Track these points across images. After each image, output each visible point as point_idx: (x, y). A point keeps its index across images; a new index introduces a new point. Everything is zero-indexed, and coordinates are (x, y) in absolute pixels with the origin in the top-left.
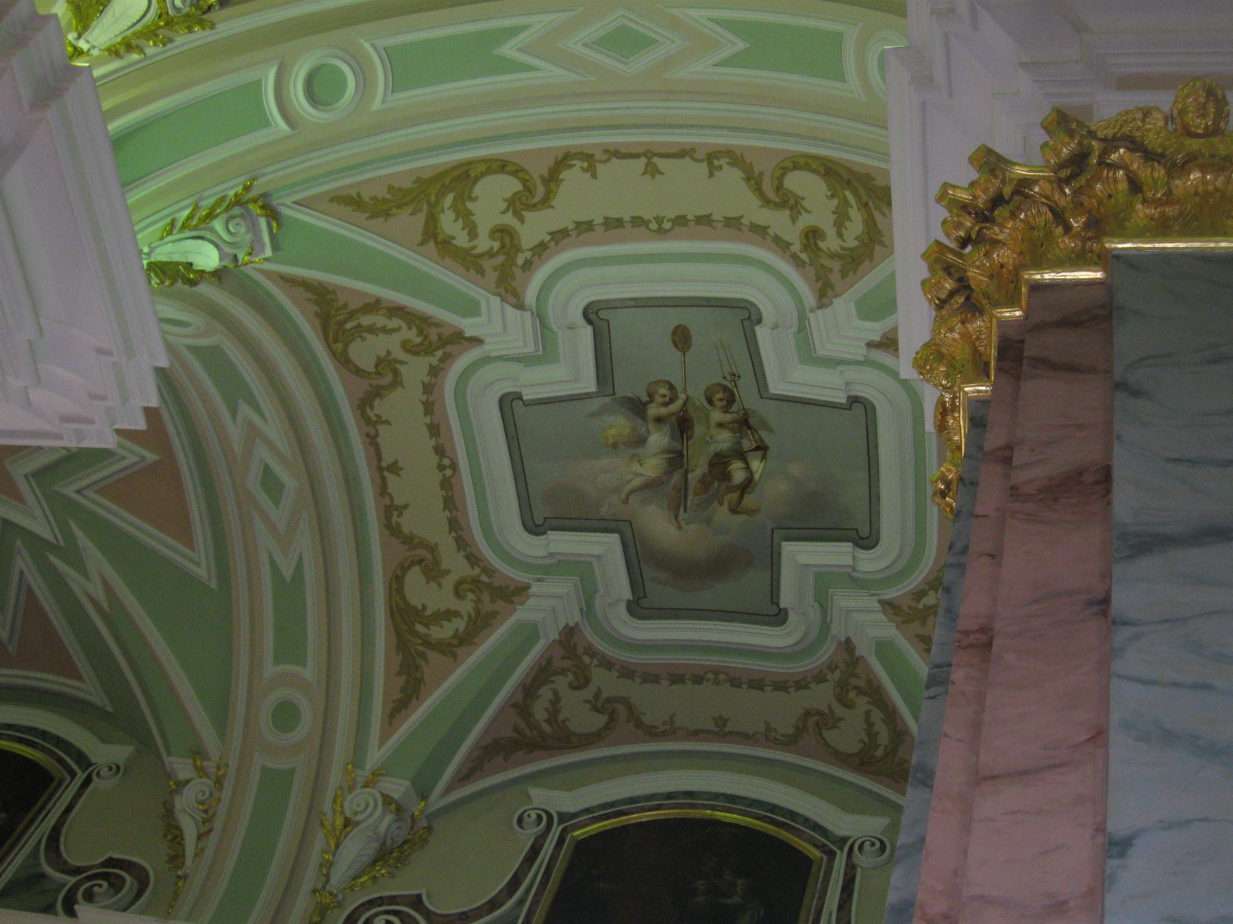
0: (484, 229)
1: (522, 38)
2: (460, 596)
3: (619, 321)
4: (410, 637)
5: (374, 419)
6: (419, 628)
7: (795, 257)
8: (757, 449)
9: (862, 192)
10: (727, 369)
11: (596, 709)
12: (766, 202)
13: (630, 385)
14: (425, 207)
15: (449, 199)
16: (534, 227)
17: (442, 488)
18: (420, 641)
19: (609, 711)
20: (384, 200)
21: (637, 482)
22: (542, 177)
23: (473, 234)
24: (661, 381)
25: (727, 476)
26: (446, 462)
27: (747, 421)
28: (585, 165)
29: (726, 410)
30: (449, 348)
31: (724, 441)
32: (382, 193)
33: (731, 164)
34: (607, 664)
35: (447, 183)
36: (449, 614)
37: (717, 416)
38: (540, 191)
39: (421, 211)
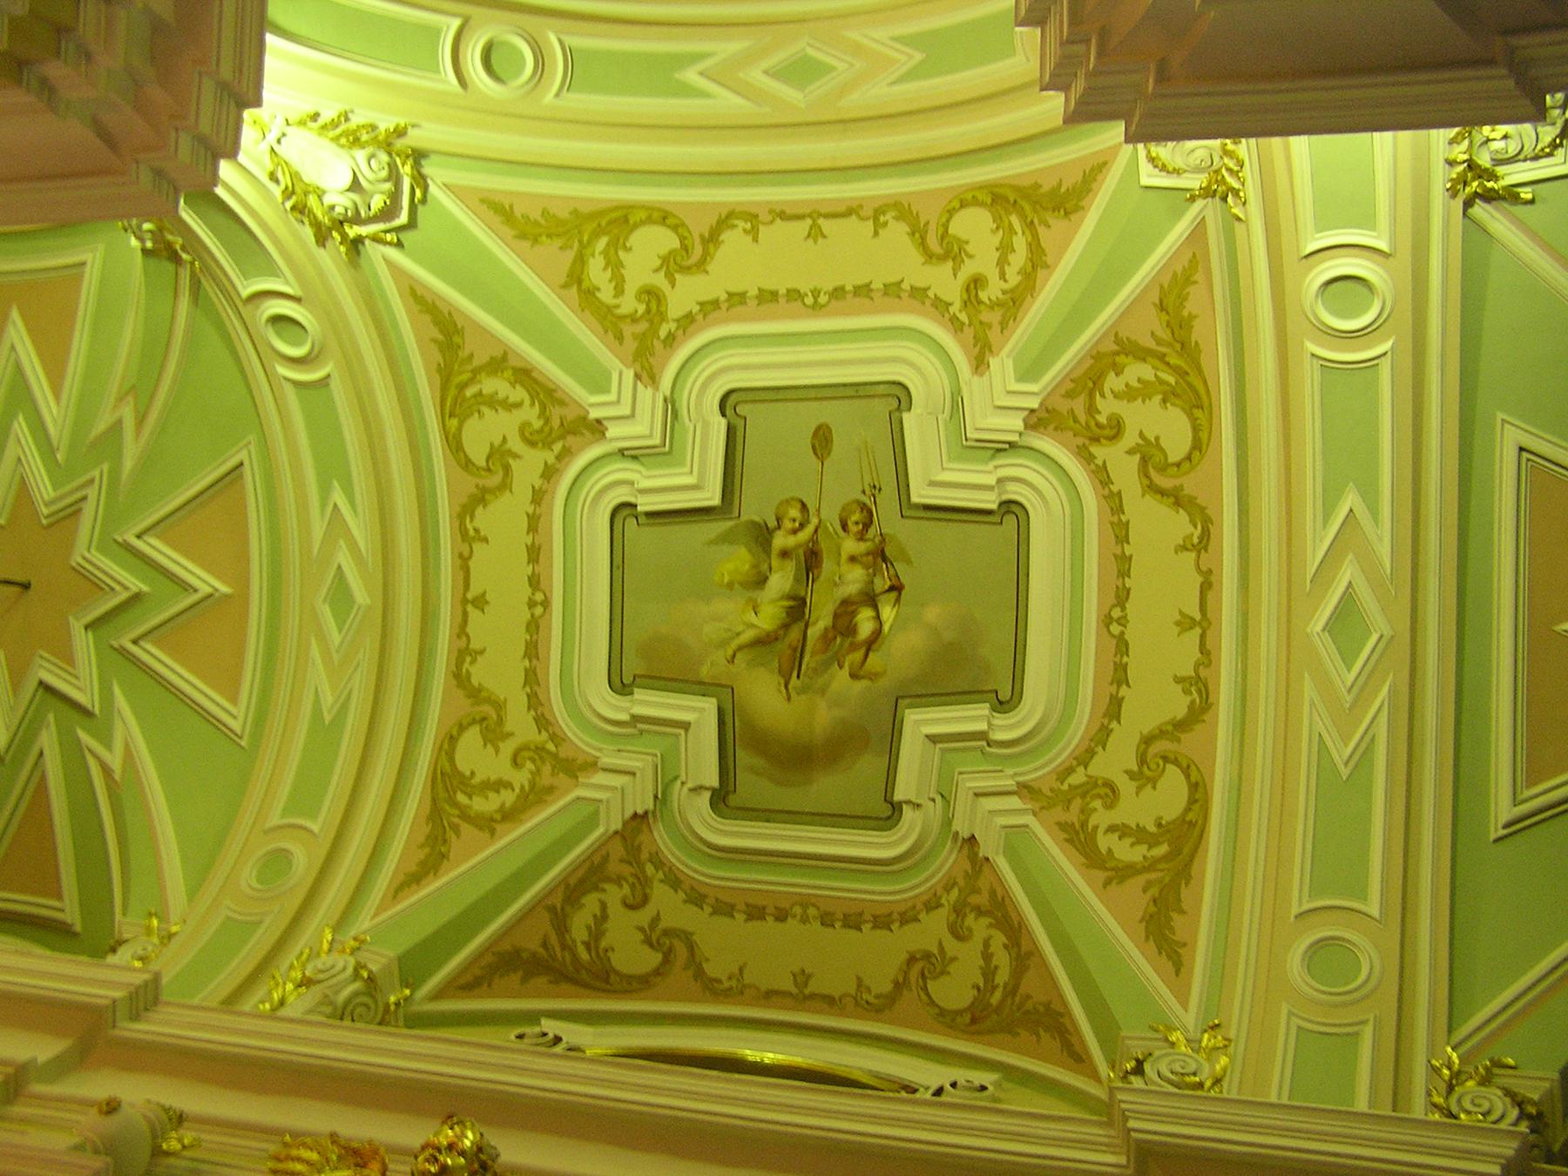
0: (631, 288)
1: (702, 66)
2: (516, 764)
3: (755, 416)
4: (447, 807)
5: (472, 533)
6: (461, 798)
7: (954, 319)
8: (892, 589)
9: (1028, 208)
10: (867, 479)
11: (648, 942)
12: (930, 256)
13: (754, 507)
14: (576, 245)
15: (603, 242)
16: (683, 296)
17: (528, 630)
18: (457, 812)
19: (665, 949)
20: (536, 223)
21: (748, 635)
22: (702, 236)
23: (619, 291)
24: (792, 499)
25: (852, 630)
26: (539, 597)
27: (883, 551)
28: (748, 226)
29: (861, 537)
30: (570, 440)
31: (854, 579)
32: (536, 215)
33: (896, 218)
34: (674, 881)
35: (603, 223)
36: (500, 785)
37: (850, 546)
38: (698, 251)
39: (571, 248)
